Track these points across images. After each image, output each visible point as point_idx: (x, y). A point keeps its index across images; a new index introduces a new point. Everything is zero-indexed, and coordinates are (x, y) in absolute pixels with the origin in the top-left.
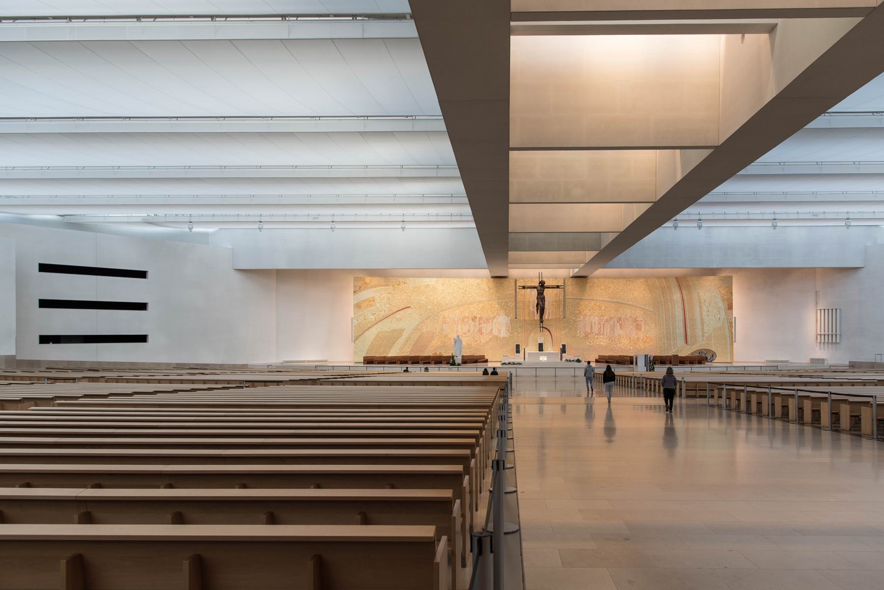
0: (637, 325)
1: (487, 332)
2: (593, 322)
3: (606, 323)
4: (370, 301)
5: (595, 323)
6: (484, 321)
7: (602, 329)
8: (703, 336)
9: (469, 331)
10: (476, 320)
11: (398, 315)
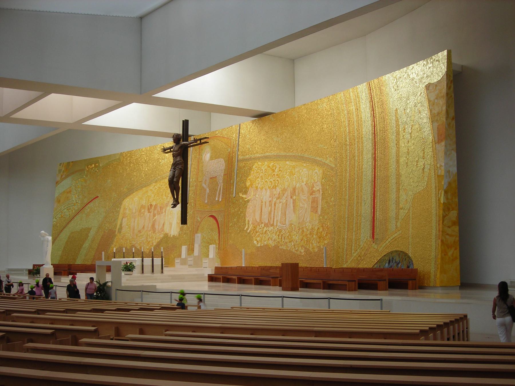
0: (313, 202)
1: (160, 228)
2: (264, 201)
3: (278, 201)
4: (68, 193)
5: (265, 202)
6: (158, 211)
7: (273, 213)
8: (397, 218)
9: (144, 227)
10: (151, 211)
11: (87, 209)
